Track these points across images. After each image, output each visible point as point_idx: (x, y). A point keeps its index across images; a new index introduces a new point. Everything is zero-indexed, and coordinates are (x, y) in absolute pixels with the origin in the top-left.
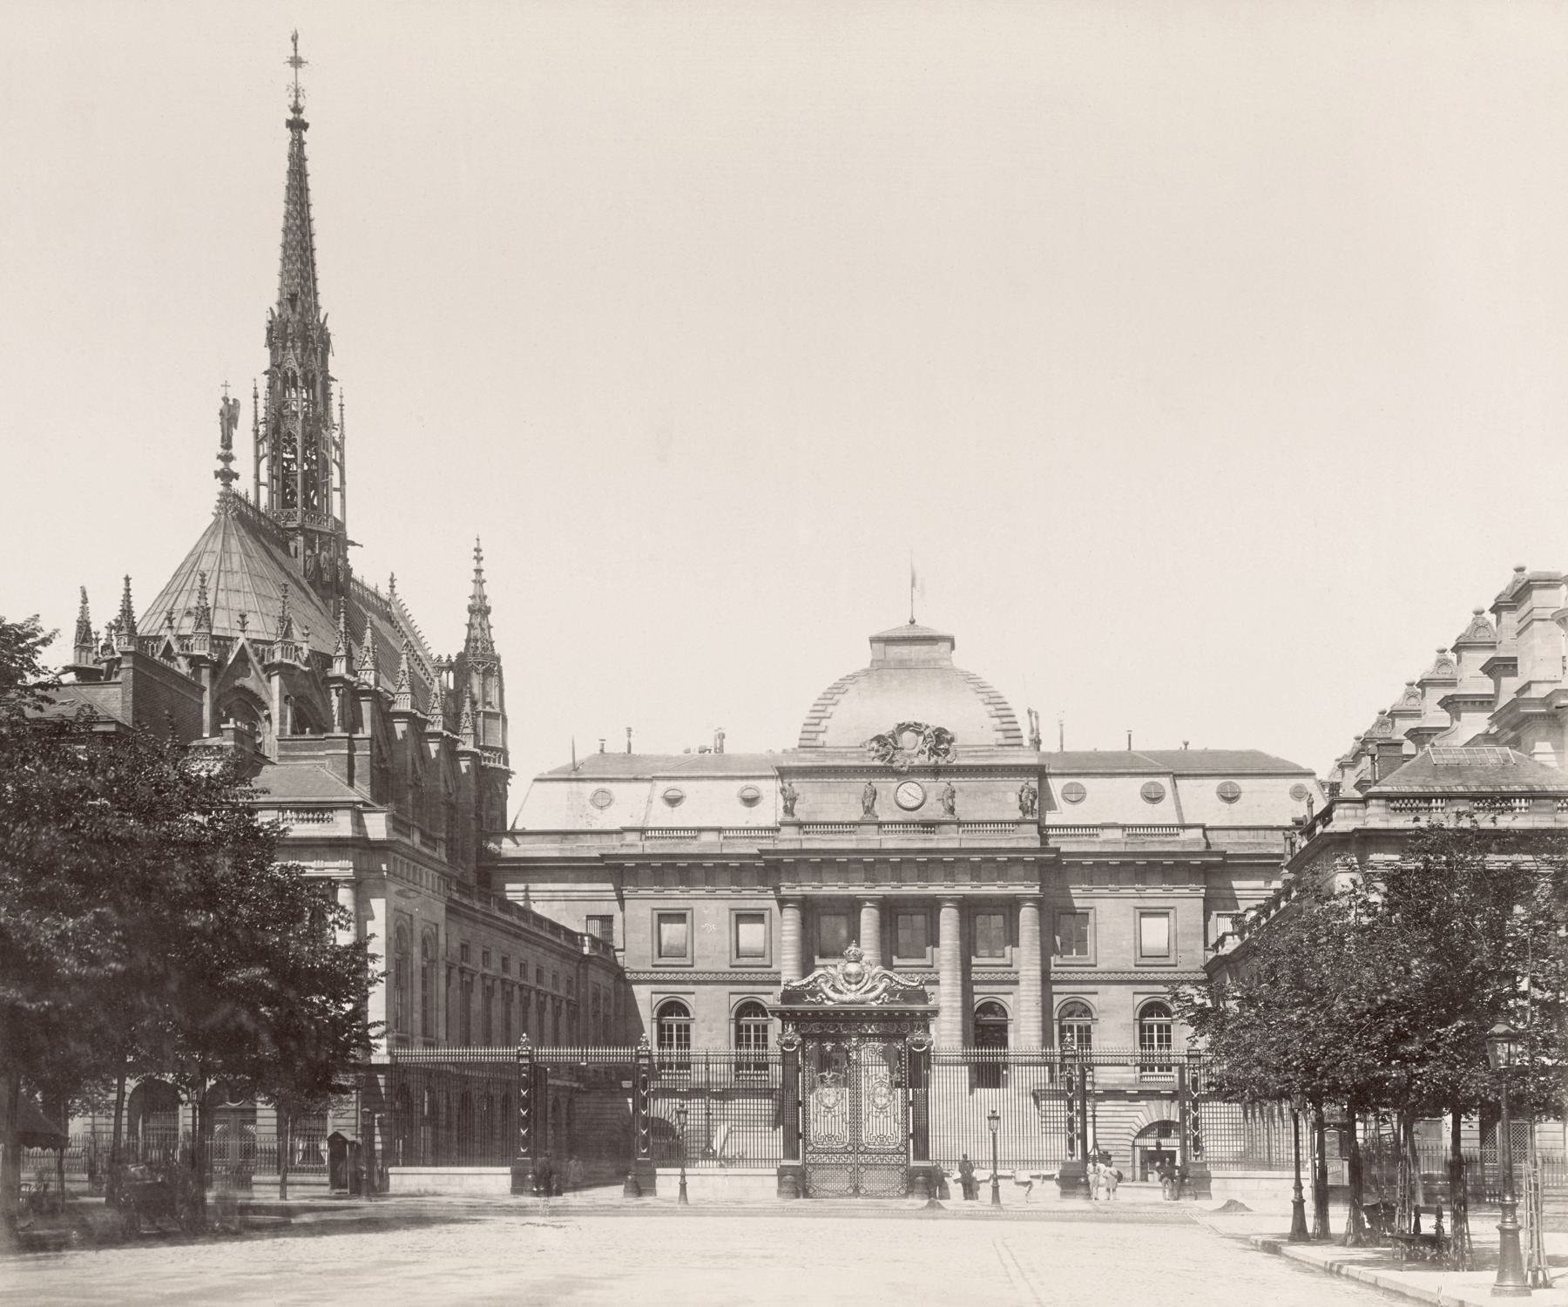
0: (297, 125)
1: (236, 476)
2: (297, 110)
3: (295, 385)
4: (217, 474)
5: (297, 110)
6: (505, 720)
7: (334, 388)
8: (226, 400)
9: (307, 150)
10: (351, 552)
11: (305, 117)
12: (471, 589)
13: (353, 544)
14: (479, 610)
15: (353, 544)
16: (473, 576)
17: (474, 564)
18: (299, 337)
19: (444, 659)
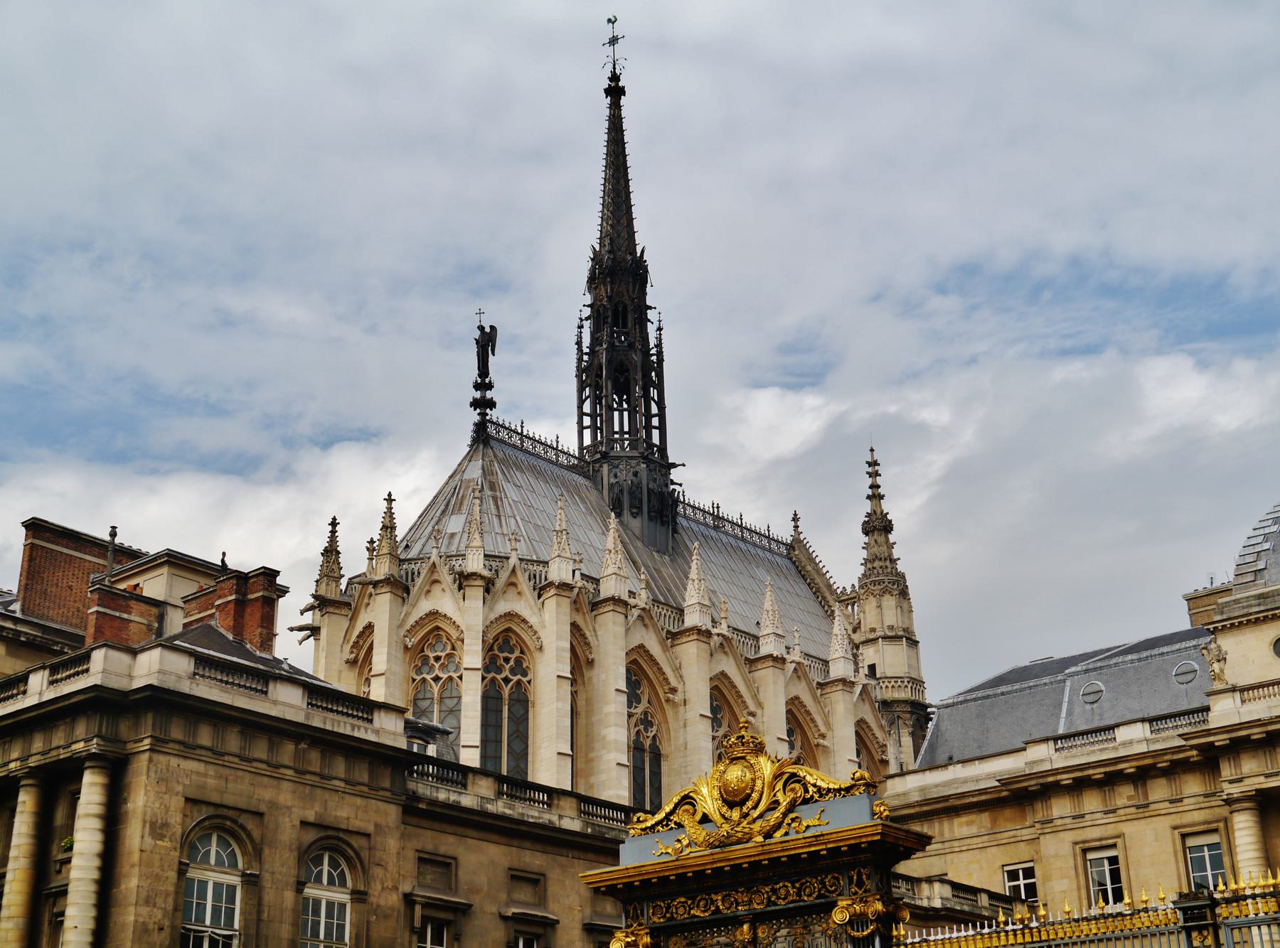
0: (615, 92)
1: (491, 404)
2: (615, 78)
4: (475, 404)
5: (615, 78)
6: (913, 643)
7: (651, 314)
8: (481, 328)
9: (624, 112)
10: (675, 475)
11: (621, 84)
12: (867, 507)
13: (674, 465)
14: (878, 526)
15: (674, 465)
16: (870, 492)
17: (870, 481)
18: (619, 278)
19: (849, 591)
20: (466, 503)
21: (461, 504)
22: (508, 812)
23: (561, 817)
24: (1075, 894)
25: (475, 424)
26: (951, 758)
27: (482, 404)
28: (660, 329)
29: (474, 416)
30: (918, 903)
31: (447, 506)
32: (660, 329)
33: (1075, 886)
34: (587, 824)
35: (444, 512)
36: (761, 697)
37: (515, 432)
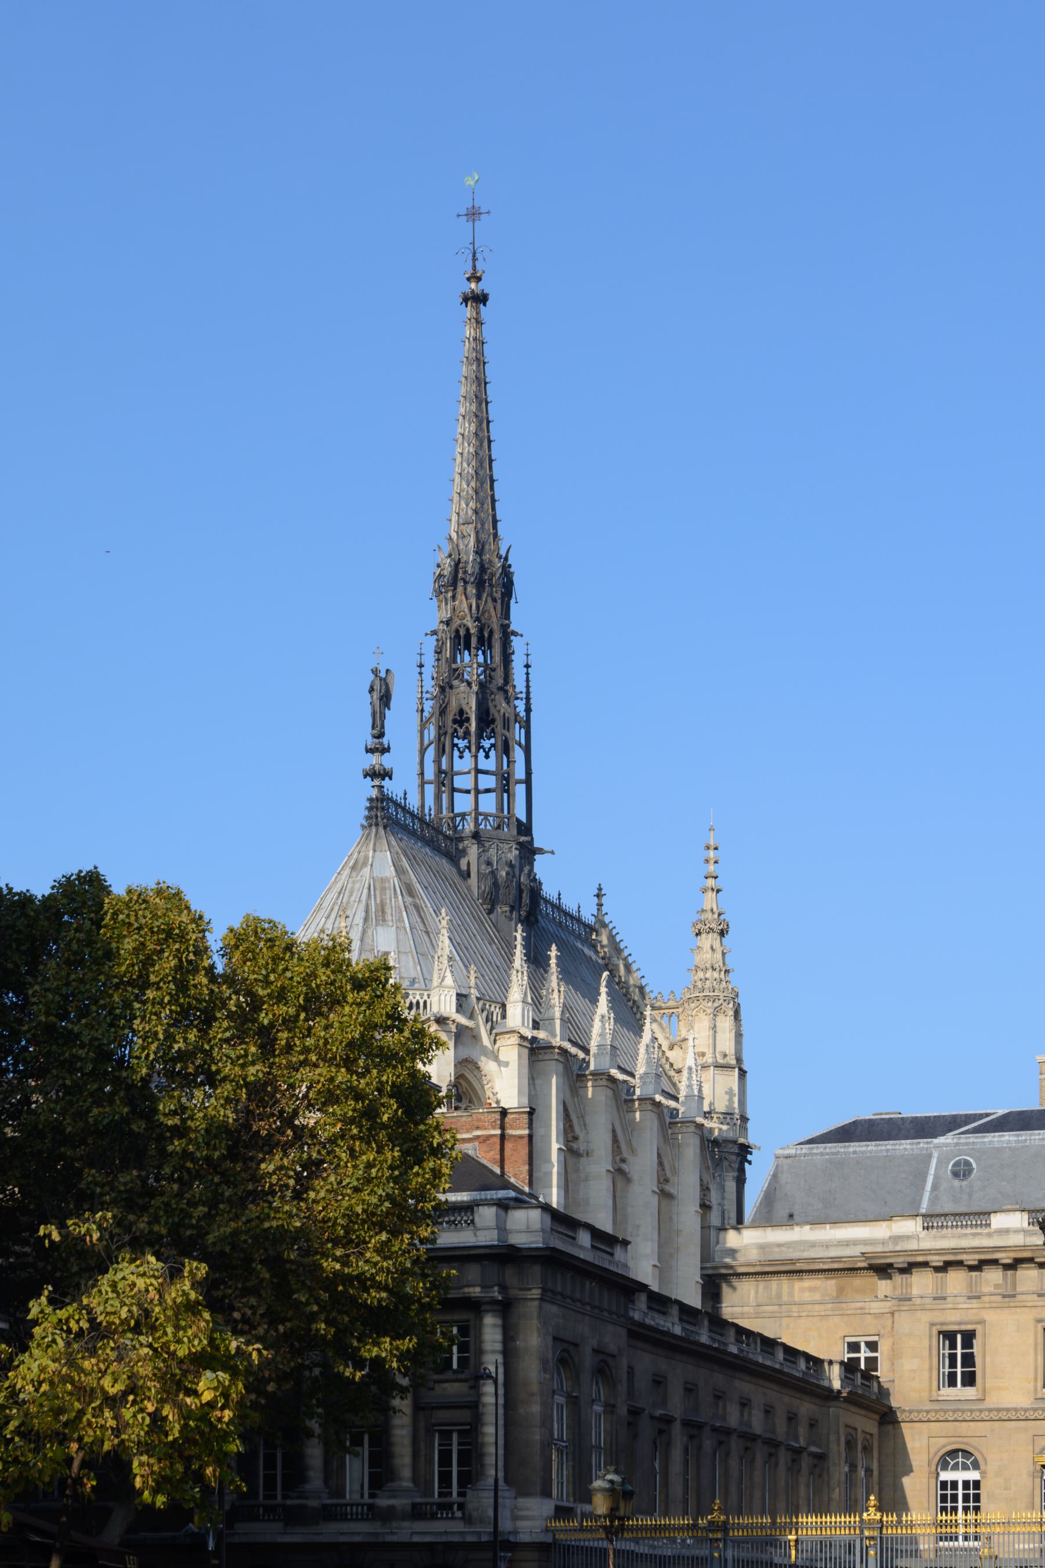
3: (468, 647)
20: (388, 911)
21: (383, 912)
22: (652, 1323)
23: (673, 1324)
24: (926, 1374)
25: (371, 800)
26: (791, 1216)
27: (380, 774)
28: (527, 666)
29: (368, 789)
30: (821, 1383)
31: (367, 911)
32: (527, 666)
33: (927, 1366)
34: (683, 1329)
35: (366, 920)
36: (634, 1143)
37: (401, 807)
